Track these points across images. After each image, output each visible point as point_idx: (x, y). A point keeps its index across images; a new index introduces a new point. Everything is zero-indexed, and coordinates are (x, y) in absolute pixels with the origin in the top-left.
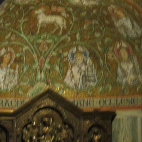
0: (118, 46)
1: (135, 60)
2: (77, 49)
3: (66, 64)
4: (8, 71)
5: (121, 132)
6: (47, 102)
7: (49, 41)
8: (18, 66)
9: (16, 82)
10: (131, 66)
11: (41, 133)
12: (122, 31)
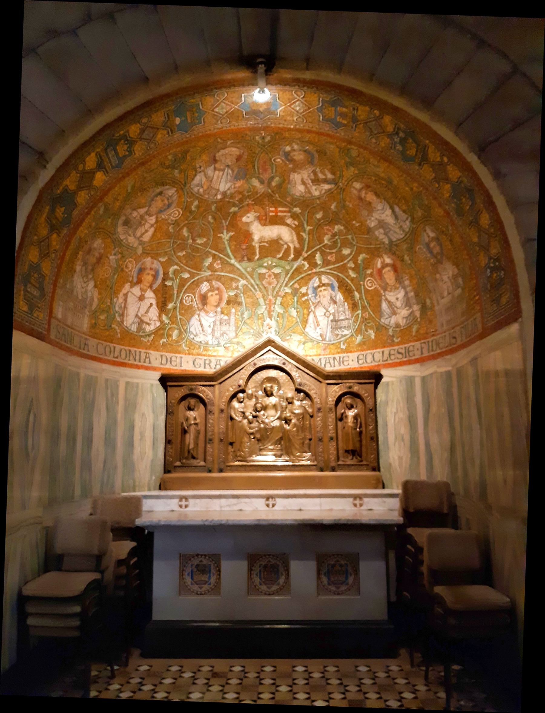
0: (379, 265)
1: (407, 283)
2: (320, 279)
3: (306, 305)
4: (218, 319)
5: (390, 403)
6: (271, 358)
7: (277, 271)
8: (233, 310)
9: (232, 334)
10: (401, 294)
11: (259, 405)
12: (380, 234)
